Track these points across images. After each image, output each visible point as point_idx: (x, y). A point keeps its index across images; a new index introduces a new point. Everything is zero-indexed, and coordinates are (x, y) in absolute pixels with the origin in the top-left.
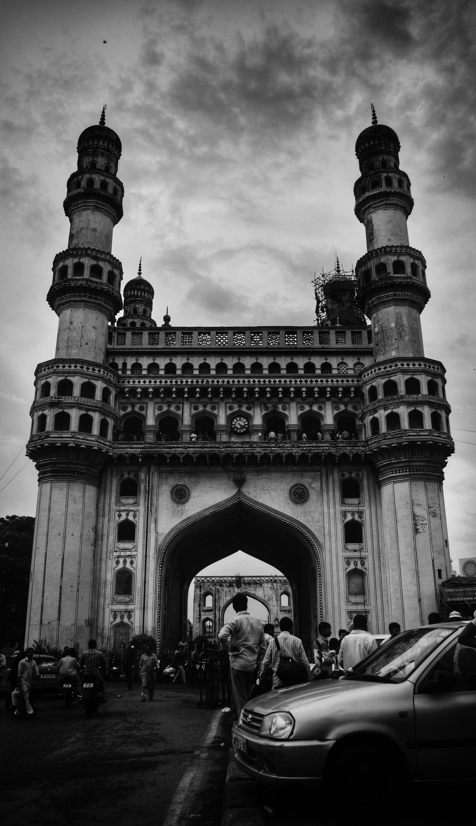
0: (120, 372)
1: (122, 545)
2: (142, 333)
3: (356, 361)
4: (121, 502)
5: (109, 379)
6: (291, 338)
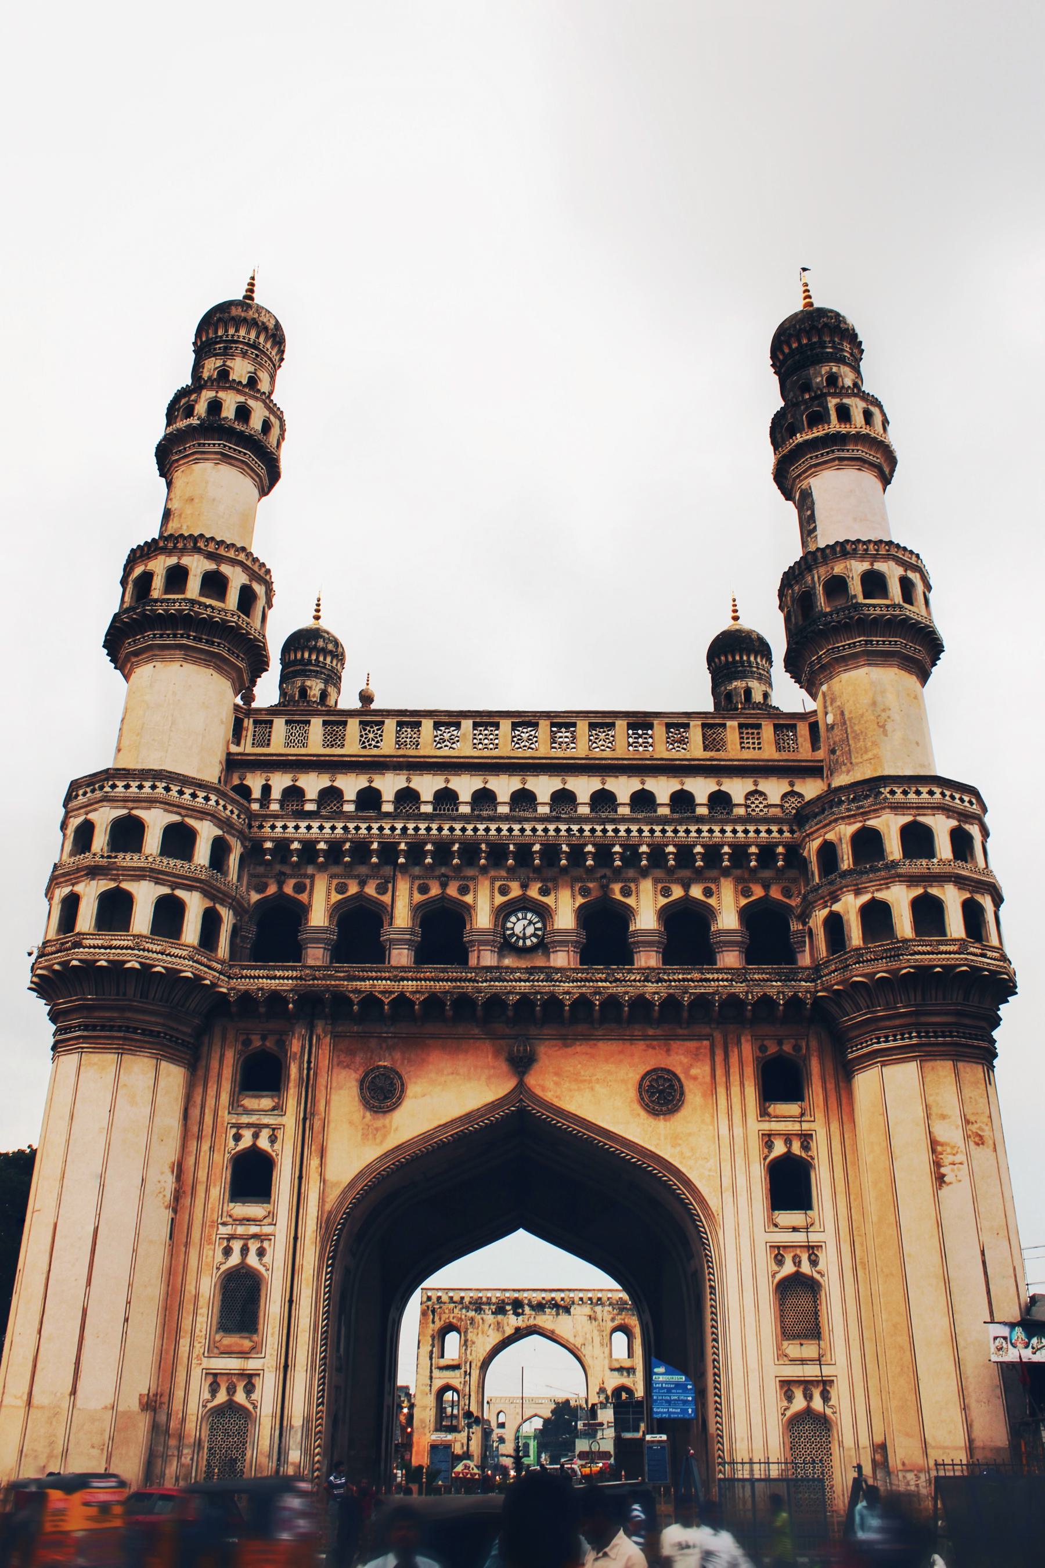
0: (255, 806)
1: (241, 1210)
2: (308, 722)
4: (242, 1106)
5: (228, 818)
6: (640, 736)
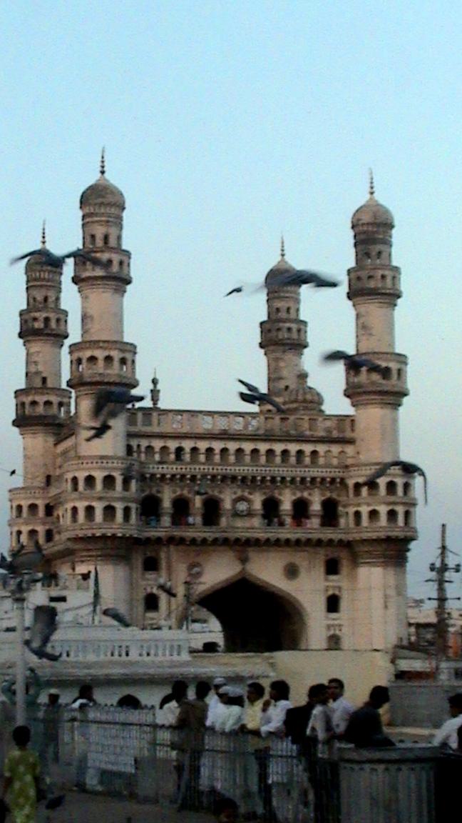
1: (150, 615)
2: (150, 414)
3: (340, 450)
